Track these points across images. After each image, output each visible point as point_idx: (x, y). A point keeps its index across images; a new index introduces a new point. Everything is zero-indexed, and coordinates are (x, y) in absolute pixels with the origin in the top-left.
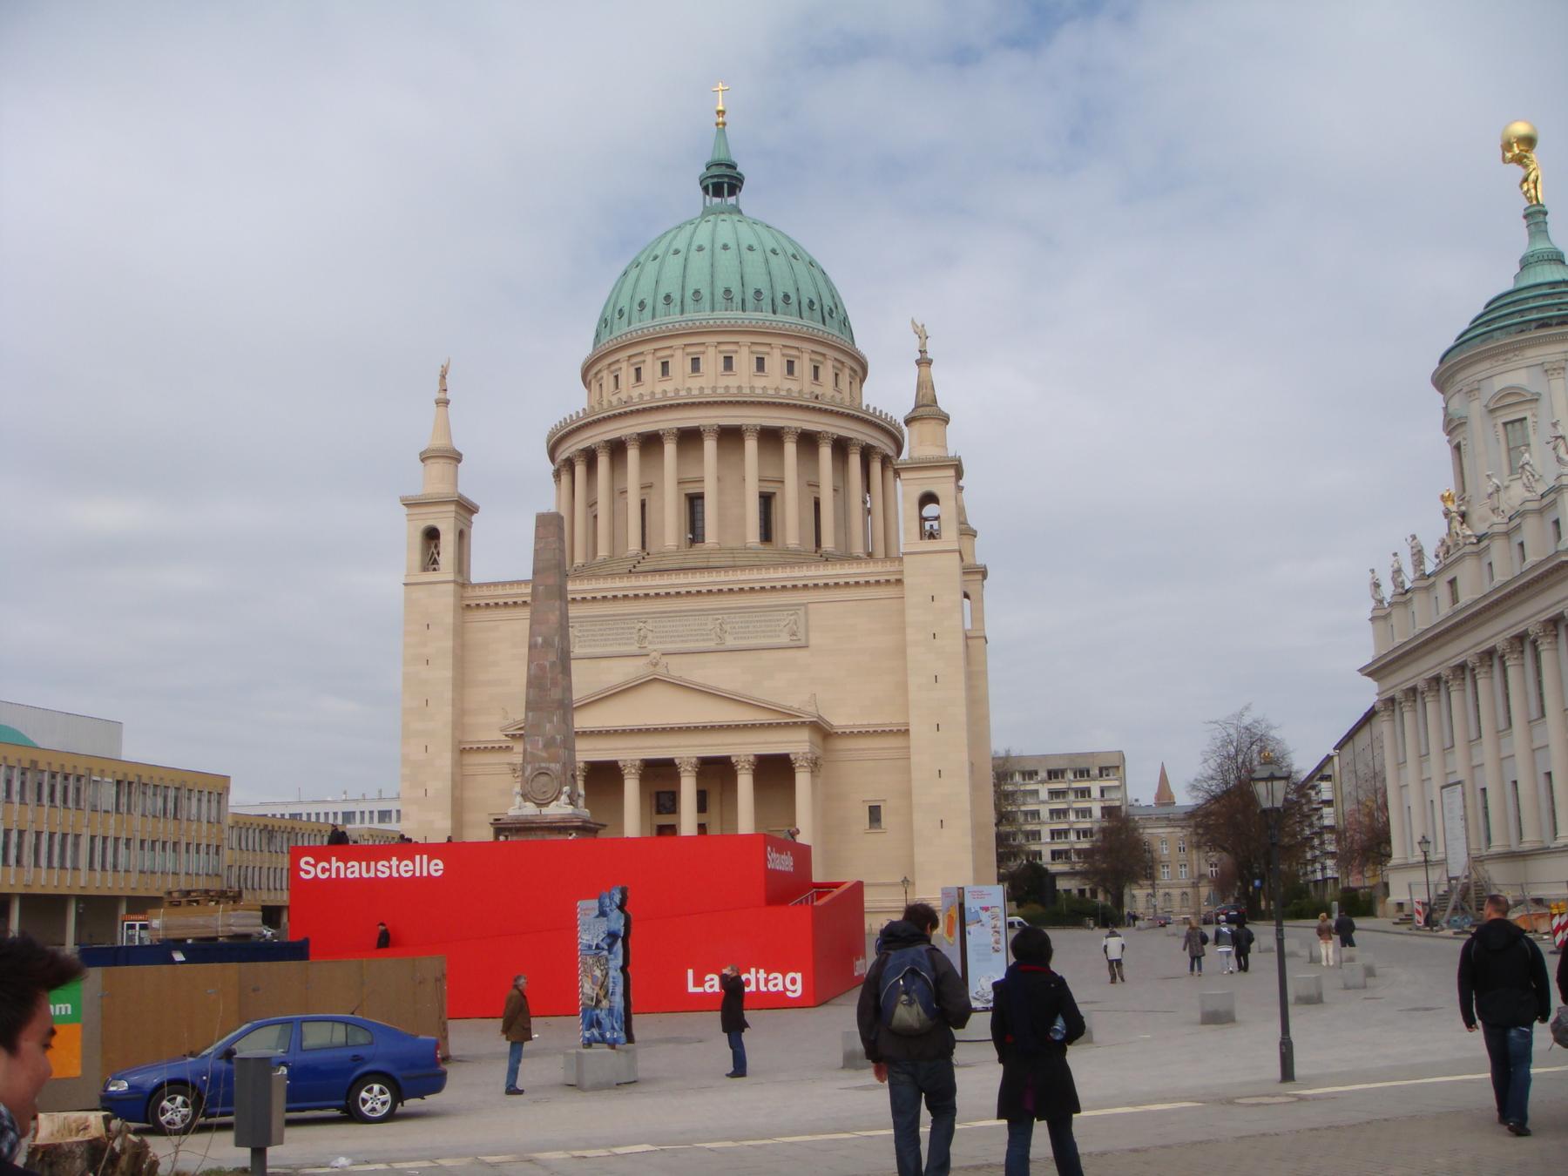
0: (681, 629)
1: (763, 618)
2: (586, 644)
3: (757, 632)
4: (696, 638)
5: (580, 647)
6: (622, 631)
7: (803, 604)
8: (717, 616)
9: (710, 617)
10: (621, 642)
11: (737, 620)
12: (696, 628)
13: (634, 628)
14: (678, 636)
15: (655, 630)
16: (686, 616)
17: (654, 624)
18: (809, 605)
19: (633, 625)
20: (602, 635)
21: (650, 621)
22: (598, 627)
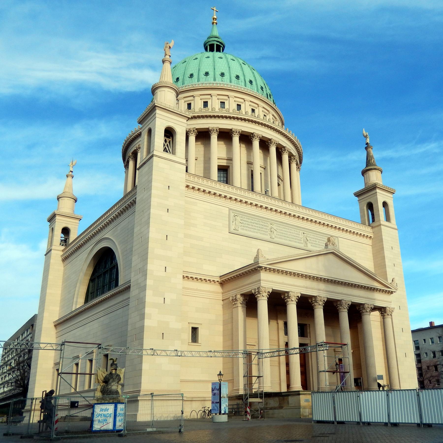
0: (289, 234)
1: (322, 239)
2: (245, 228)
3: (320, 245)
4: (296, 240)
5: (242, 229)
6: (261, 226)
7: (337, 237)
8: (305, 232)
9: (301, 232)
10: (262, 232)
11: (312, 236)
12: (295, 235)
13: (268, 227)
14: (288, 237)
15: (277, 230)
16: (291, 227)
17: (277, 227)
18: (339, 238)
19: (268, 225)
20: (252, 226)
21: (275, 225)
22: (250, 221)
